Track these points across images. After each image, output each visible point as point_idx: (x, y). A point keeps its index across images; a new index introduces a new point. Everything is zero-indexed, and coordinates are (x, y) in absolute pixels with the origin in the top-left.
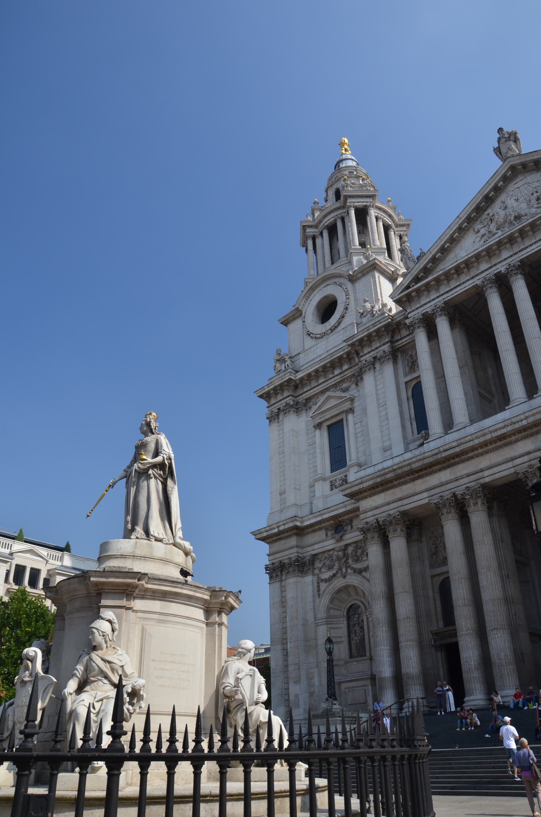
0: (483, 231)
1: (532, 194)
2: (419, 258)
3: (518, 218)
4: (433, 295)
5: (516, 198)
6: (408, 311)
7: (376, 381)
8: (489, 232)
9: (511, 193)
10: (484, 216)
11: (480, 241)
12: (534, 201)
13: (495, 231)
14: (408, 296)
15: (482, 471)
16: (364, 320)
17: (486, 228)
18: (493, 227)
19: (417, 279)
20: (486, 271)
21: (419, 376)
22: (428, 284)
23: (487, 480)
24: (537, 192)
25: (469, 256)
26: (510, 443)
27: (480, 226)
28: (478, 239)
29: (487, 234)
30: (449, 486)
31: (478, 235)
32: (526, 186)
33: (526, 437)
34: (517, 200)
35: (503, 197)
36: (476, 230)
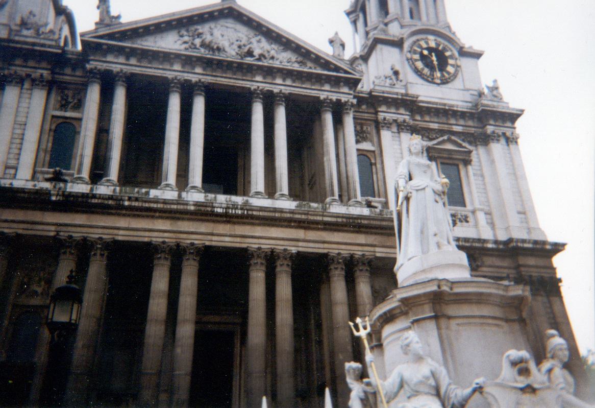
0: (186, 38)
1: (237, 41)
2: (113, 17)
3: (219, 49)
4: (122, 60)
5: (223, 34)
6: (92, 58)
7: (20, 97)
8: (192, 44)
9: (219, 26)
10: (193, 28)
11: (181, 45)
12: (235, 47)
13: (198, 46)
14: (100, 44)
15: (118, 229)
16: (25, 32)
17: (191, 38)
18: (198, 41)
19: (111, 36)
20: (174, 72)
21: (80, 120)
22: (123, 48)
23: (120, 238)
24: (241, 41)
25: (171, 51)
26: (153, 217)
27: (185, 33)
28: (180, 42)
29: (190, 44)
30: (79, 229)
31: (181, 39)
32: (233, 30)
33: (167, 218)
34: (223, 36)
35: (212, 25)
36: (181, 34)
